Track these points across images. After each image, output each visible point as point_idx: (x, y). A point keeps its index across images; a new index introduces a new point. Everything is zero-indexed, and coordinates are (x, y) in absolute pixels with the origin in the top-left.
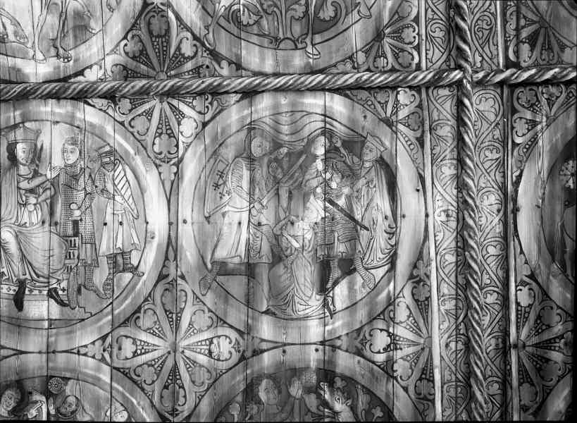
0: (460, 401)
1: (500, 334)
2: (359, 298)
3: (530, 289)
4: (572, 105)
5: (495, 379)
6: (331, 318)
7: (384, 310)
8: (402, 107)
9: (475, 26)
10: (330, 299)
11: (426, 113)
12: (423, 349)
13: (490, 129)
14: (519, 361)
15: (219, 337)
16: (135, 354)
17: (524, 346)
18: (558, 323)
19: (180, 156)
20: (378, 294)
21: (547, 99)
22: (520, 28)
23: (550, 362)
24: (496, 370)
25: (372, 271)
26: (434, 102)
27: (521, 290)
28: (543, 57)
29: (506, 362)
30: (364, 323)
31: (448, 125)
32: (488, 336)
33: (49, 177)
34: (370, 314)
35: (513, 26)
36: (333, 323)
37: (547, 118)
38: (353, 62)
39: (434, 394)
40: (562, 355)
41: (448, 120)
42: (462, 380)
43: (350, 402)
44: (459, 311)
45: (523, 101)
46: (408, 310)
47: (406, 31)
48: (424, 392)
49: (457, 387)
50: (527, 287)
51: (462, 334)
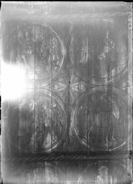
15: (80, 84)
16: (58, 89)
19: (70, 35)
25: (122, 66)
33: (34, 41)
36: (111, 80)
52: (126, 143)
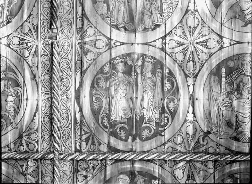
4: (103, 169)
8: (29, 168)
9: (62, 134)
11: (40, 170)
13: (67, 179)
21: (92, 166)
22: (82, 135)
26: (44, 166)
28: (91, 148)
31: (49, 176)
35: (79, 134)
37: (92, 174)
38: (9, 148)
41: (50, 174)
45: (82, 167)
47: (32, 134)
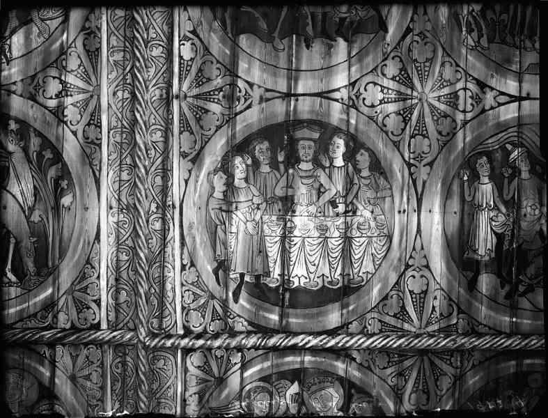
0: (125, 146)
1: (164, 85)
2: (34, 46)
3: (192, 44)
5: (159, 127)
6: (8, 65)
7: (57, 60)
10: (7, 47)
12: (92, 96)
14: (180, 114)
17: (186, 97)
18: (217, 76)
20: (51, 45)
23: (209, 113)
24: (160, 119)
25: (48, 22)
27: (184, 44)
29: (169, 110)
30: (38, 71)
32: (154, 85)
34: (44, 61)
36: (10, 69)
39: (101, 139)
40: (220, 106)
42: (127, 126)
43: (22, 144)
44: (127, 63)
46: (79, 60)
48: (92, 136)
49: (122, 133)
50: (190, 42)
51: (130, 84)
52: (53, 293)
